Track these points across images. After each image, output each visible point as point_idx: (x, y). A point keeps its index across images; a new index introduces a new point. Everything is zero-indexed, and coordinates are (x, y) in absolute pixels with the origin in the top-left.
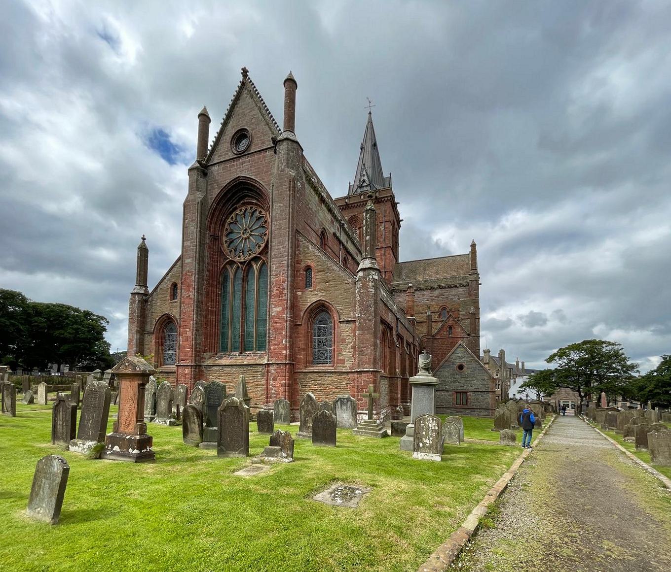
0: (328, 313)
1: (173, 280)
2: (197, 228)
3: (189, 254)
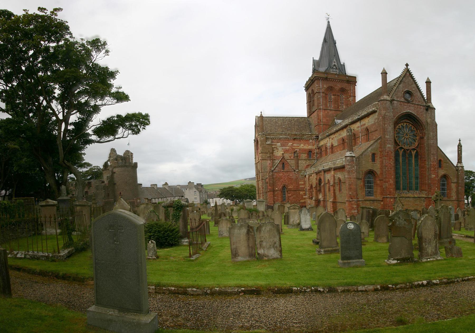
0: (446, 179)
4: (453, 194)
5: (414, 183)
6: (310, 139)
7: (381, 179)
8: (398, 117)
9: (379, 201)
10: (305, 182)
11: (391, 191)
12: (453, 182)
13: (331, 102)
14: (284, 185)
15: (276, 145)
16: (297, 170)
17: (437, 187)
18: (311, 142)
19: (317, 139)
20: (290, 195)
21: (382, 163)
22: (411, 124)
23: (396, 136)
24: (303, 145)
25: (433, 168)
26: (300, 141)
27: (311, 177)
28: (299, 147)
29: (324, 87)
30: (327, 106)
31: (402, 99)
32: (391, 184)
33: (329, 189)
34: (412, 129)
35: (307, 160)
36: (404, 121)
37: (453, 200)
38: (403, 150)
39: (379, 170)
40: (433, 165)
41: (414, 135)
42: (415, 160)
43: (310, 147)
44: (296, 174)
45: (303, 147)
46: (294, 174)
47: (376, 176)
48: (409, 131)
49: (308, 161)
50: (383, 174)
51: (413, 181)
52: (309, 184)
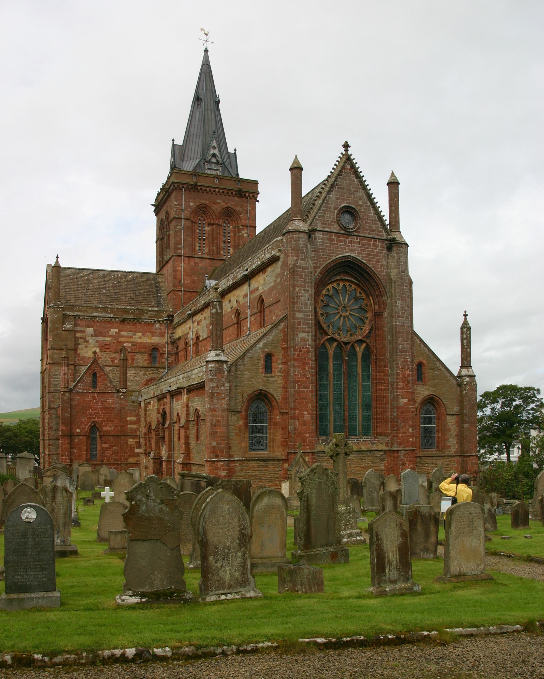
1: (267, 350)
2: (311, 301)
3: (303, 328)
4: (451, 440)
5: (360, 418)
6: (155, 322)
7: (285, 411)
8: (324, 268)
9: (279, 460)
10: (138, 415)
11: (307, 437)
12: (451, 413)
13: (204, 240)
15: (83, 332)
16: (124, 391)
17: (412, 426)
18: (157, 329)
20: (106, 445)
21: (286, 374)
22: (356, 284)
23: (319, 311)
25: (403, 382)
26: (134, 324)
27: (150, 406)
28: (132, 337)
29: (190, 207)
30: (195, 249)
31: (335, 228)
32: (305, 423)
33: (179, 434)
34: (358, 294)
35: (147, 368)
36: (338, 278)
37: (450, 454)
38: (335, 344)
39: (280, 390)
40: (404, 375)
41: (361, 308)
42: (362, 366)
43: (155, 340)
44: (121, 399)
45: (140, 338)
46: (118, 397)
47: (273, 404)
48: (349, 300)
49: (149, 370)
50: (290, 400)
51: (359, 414)
52: (146, 421)
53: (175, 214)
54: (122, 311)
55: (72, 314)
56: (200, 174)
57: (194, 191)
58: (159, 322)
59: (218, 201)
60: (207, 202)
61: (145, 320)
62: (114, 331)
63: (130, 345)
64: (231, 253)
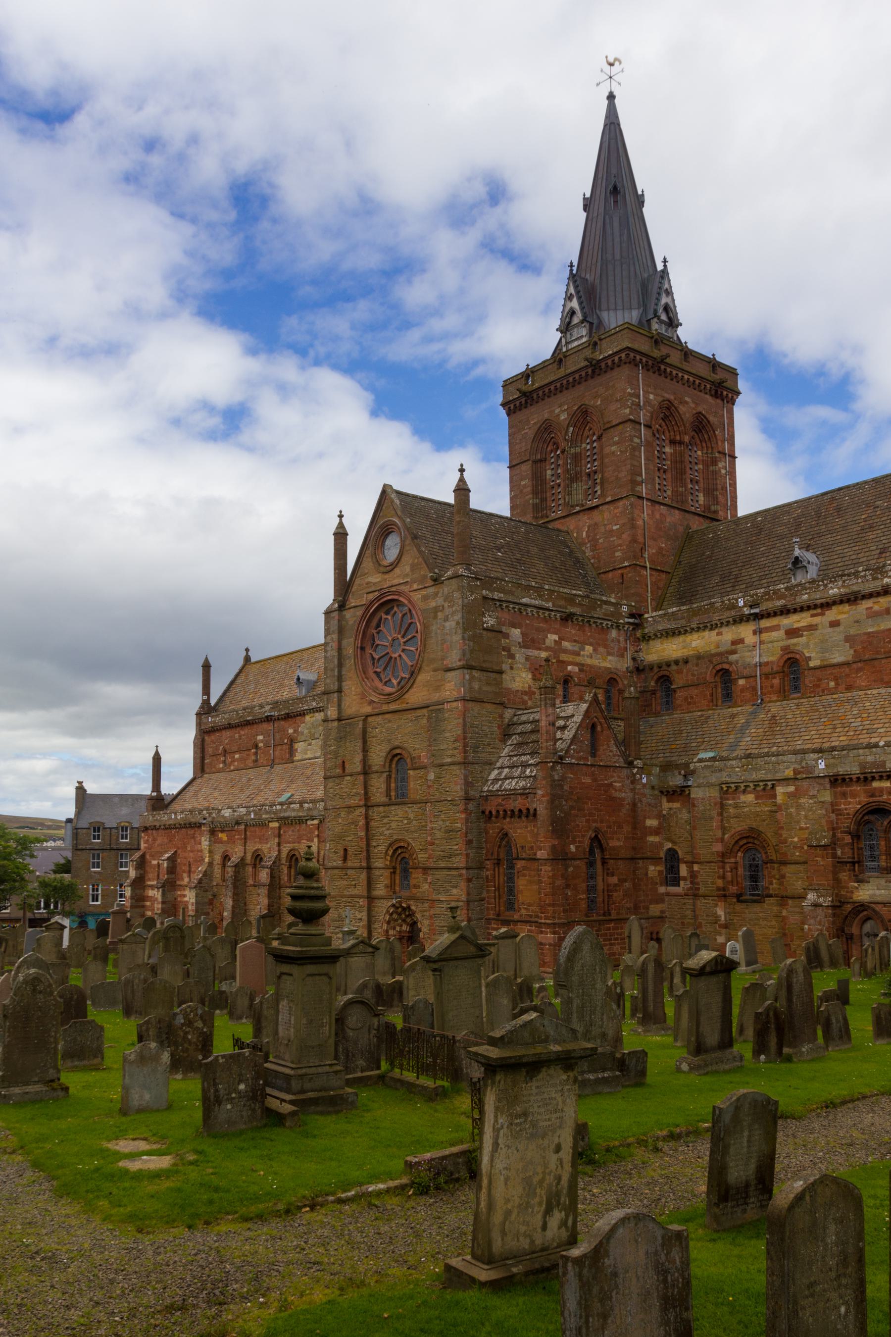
14: (597, 830)
18: (613, 641)
19: (634, 629)
24: (591, 648)
28: (578, 654)
53: (631, 414)
54: (566, 599)
55: (490, 595)
56: (665, 341)
57: (654, 373)
58: (618, 627)
59: (687, 399)
60: (672, 398)
61: (600, 621)
62: (552, 637)
63: (576, 669)
64: (701, 502)
